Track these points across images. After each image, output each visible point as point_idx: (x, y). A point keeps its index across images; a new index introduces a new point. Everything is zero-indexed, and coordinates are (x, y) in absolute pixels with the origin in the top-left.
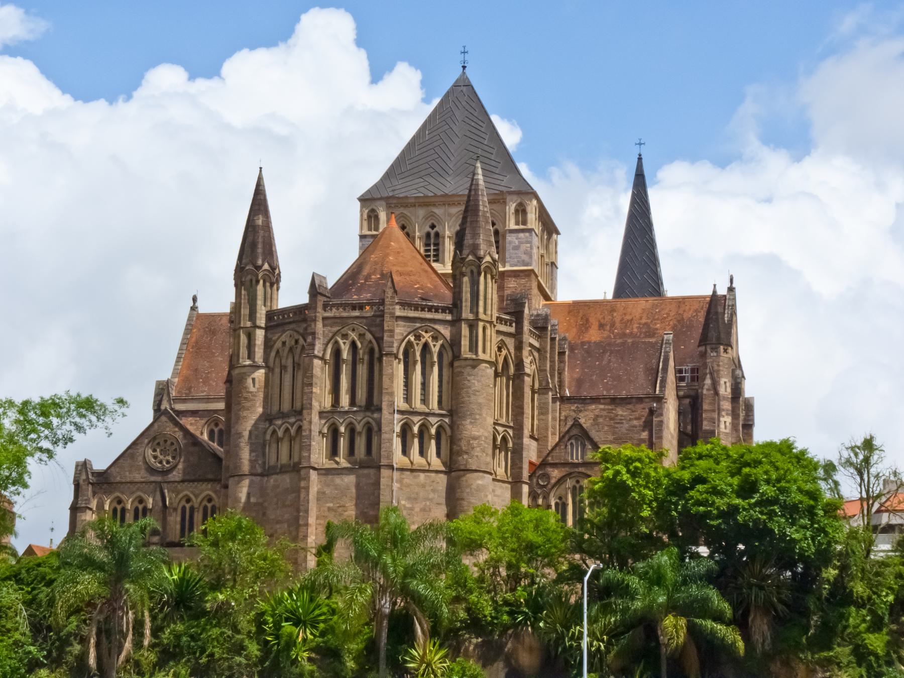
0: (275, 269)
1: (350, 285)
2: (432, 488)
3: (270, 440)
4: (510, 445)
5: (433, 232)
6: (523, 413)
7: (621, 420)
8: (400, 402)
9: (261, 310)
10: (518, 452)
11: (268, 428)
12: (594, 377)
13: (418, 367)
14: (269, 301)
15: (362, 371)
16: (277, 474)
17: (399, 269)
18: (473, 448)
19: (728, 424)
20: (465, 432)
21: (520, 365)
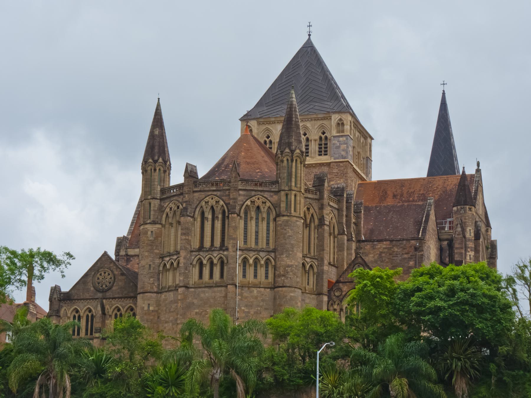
0: (167, 162)
1: (217, 171)
2: (262, 298)
3: (163, 270)
4: (316, 270)
6: (323, 250)
7: (397, 254)
8: (240, 243)
9: (157, 188)
10: (319, 275)
11: (161, 263)
12: (381, 228)
13: (253, 222)
14: (162, 182)
15: (218, 225)
16: (166, 292)
17: (248, 160)
18: (288, 273)
19: (472, 256)
20: (282, 263)
21: (322, 220)
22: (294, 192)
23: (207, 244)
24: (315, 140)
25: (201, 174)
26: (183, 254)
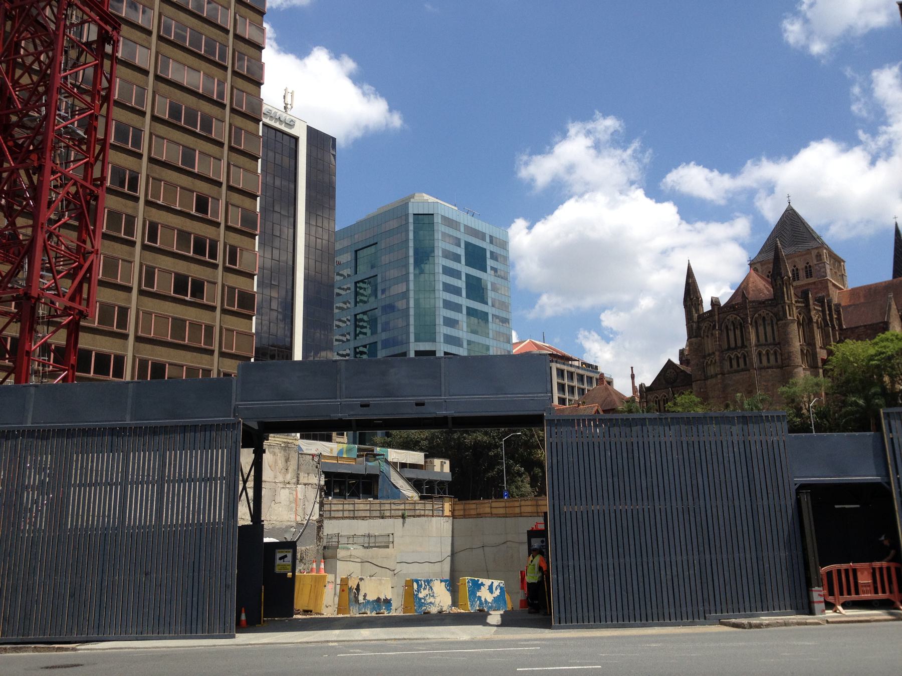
15: (738, 332)
23: (733, 345)
24: (802, 269)
25: (723, 303)
26: (717, 353)
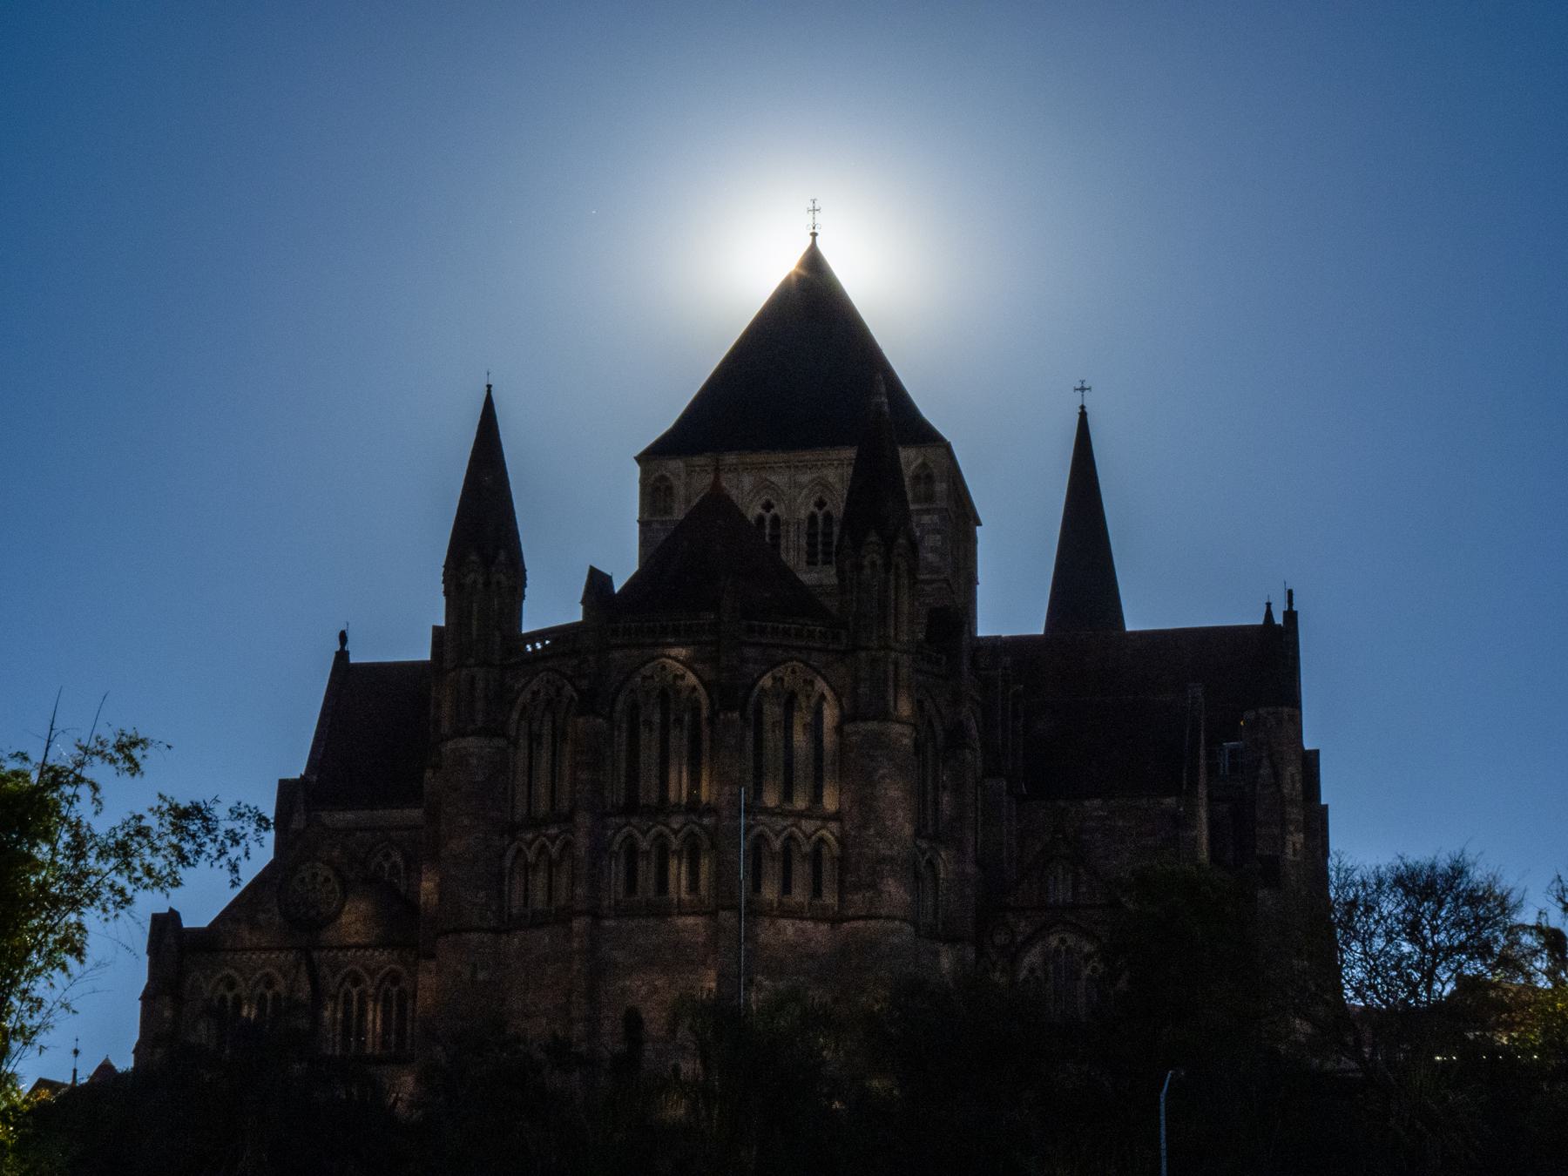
5: (768, 516)
19: (1298, 846)
22: (893, 655)
26: (583, 819)
